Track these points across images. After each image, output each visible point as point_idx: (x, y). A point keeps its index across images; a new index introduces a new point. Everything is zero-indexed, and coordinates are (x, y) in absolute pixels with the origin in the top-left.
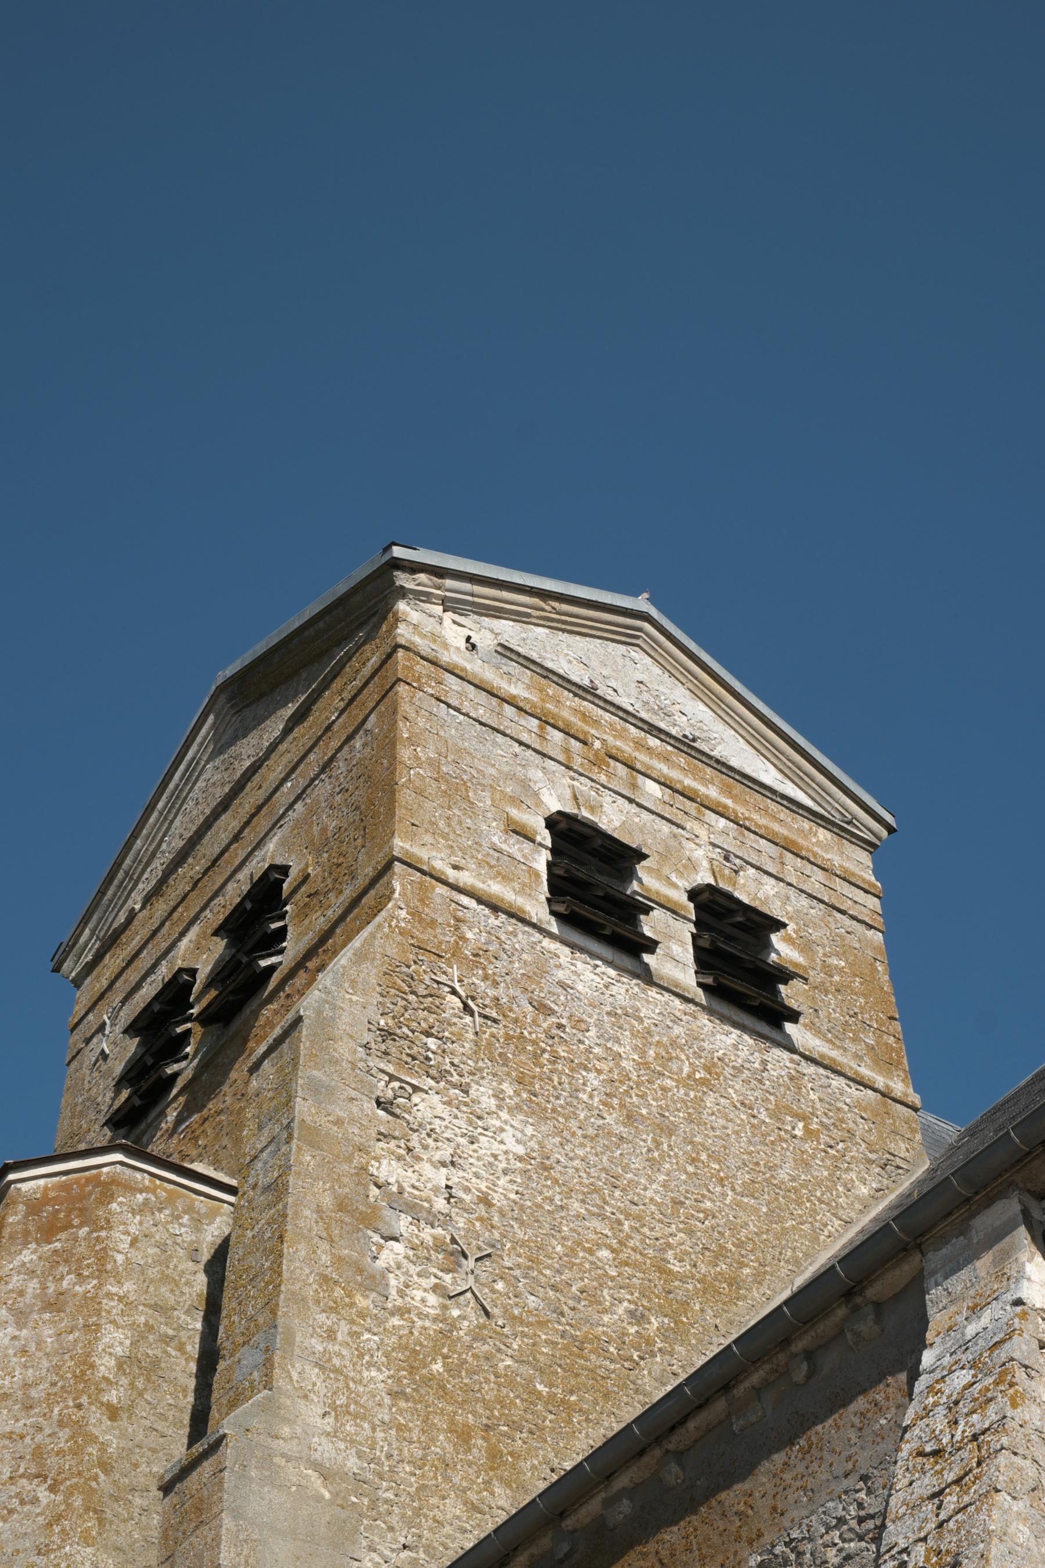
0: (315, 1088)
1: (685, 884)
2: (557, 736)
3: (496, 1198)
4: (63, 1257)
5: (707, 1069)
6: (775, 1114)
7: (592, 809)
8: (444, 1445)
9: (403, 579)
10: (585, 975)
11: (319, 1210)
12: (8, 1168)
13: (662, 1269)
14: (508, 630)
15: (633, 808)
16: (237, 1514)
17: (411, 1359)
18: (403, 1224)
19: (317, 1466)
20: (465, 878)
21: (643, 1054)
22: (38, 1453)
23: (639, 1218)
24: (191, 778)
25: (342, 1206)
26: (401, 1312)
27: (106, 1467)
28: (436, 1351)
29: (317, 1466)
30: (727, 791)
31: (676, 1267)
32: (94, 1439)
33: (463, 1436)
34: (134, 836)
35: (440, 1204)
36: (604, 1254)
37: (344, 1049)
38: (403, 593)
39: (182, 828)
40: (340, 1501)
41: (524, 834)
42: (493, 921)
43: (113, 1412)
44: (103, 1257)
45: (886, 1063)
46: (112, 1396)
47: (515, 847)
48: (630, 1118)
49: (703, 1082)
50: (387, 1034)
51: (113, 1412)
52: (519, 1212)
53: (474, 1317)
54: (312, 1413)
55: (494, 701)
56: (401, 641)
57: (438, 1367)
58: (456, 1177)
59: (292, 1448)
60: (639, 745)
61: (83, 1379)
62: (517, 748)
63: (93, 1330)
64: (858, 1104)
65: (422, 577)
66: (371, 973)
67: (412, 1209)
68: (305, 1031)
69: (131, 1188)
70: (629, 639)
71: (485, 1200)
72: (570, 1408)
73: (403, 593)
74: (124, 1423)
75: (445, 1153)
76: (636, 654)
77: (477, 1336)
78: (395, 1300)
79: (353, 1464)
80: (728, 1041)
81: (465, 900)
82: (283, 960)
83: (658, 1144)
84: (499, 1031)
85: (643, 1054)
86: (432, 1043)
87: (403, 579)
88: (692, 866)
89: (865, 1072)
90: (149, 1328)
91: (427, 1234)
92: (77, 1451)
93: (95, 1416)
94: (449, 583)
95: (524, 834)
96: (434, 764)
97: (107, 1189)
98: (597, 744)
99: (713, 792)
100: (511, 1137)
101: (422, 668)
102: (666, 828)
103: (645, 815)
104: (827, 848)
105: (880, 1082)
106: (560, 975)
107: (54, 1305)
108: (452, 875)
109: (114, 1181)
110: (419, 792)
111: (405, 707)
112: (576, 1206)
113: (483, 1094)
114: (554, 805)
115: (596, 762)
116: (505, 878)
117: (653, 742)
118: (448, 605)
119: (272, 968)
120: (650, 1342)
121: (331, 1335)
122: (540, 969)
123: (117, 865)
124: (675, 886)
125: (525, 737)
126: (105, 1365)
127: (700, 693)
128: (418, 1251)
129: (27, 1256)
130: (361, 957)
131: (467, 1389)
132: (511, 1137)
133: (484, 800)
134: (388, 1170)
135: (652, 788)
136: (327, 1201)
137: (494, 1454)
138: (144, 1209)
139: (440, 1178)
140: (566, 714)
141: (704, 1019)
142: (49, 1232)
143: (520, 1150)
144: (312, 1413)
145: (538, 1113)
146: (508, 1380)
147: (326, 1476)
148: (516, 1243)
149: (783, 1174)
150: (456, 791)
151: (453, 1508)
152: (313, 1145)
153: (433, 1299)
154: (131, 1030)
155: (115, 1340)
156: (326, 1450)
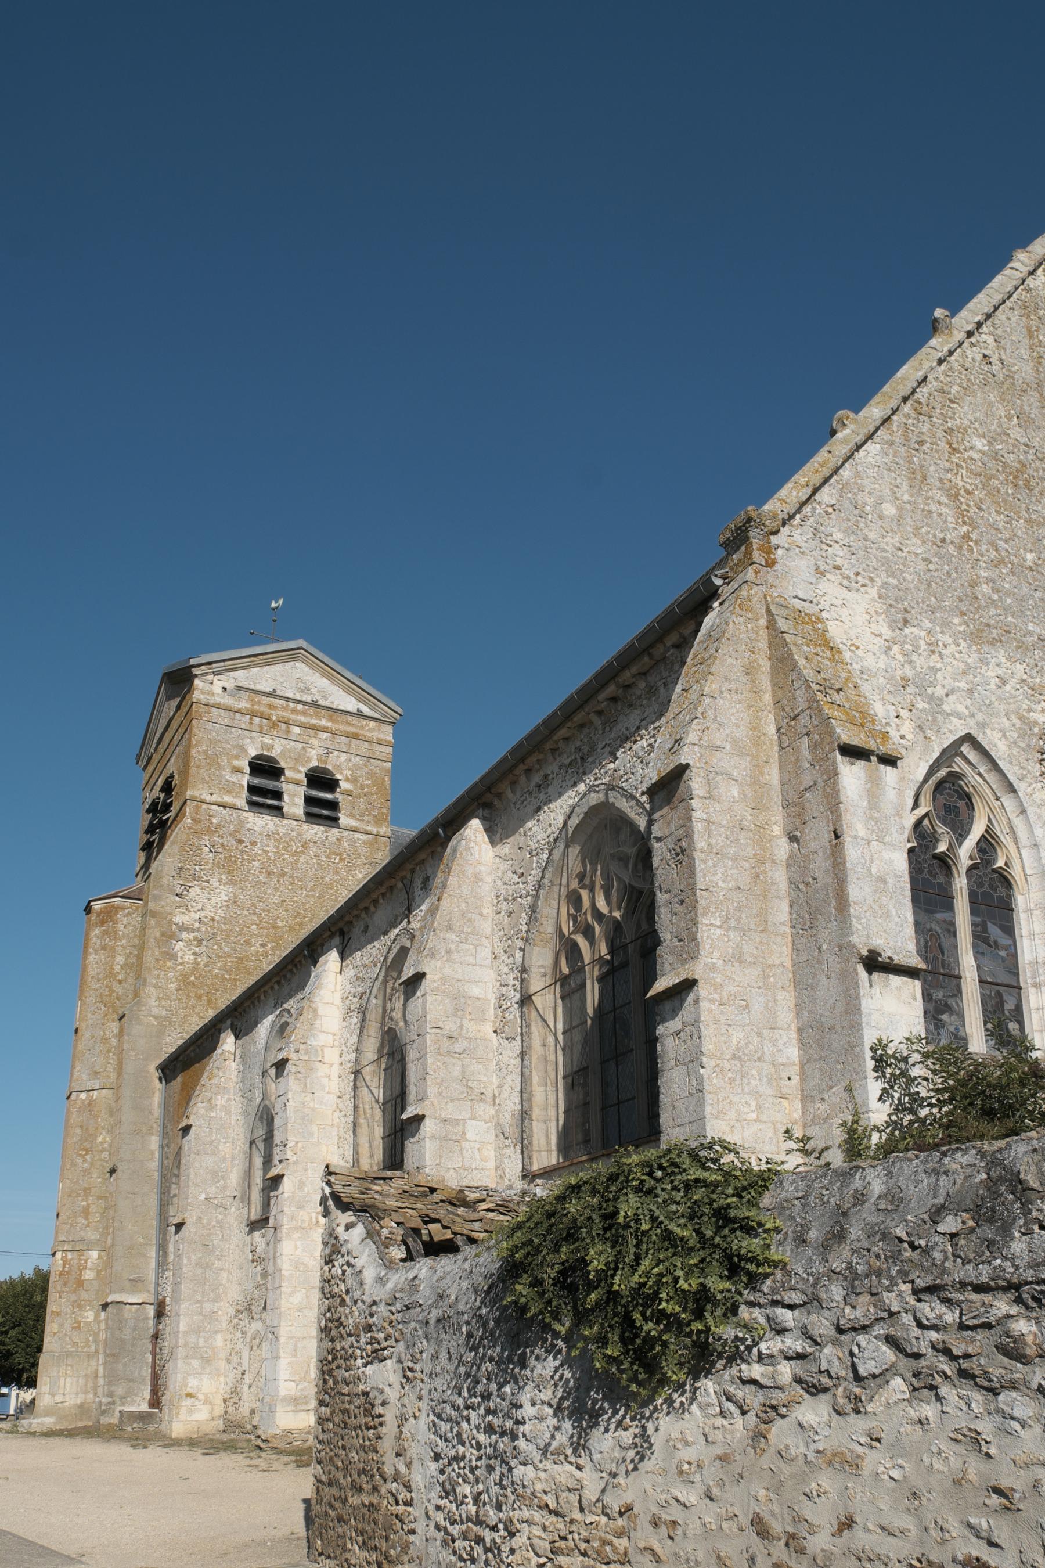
0: (155, 897)
1: (304, 770)
2: (257, 720)
3: (217, 918)
4: (105, 932)
5: (303, 846)
6: (328, 857)
7: (268, 750)
8: (193, 1001)
9: (196, 671)
10: (261, 822)
11: (155, 938)
12: (90, 902)
13: (275, 927)
14: (241, 677)
15: (287, 742)
16: (129, 1035)
17: (185, 977)
18: (184, 935)
19: (153, 1016)
20: (215, 798)
21: (278, 848)
22: (101, 995)
23: (268, 911)
24: (160, 712)
25: (163, 935)
26: (181, 964)
27: (118, 999)
28: (192, 973)
29: (153, 1016)
30: (330, 719)
31: (280, 924)
32: (114, 991)
33: (199, 997)
34: (149, 722)
35: (197, 925)
36: (254, 927)
37: (165, 881)
38: (196, 676)
39: (163, 722)
40: (160, 1024)
41: (238, 770)
42: (224, 812)
43: (120, 982)
44: (116, 933)
45: (378, 822)
46: (120, 977)
47: (234, 778)
48: (269, 874)
49: (301, 852)
50: (181, 869)
51: (120, 982)
52: (225, 920)
53: (205, 959)
54: (153, 1002)
55: (232, 714)
56: (194, 700)
57: (193, 978)
58: (203, 914)
59: (145, 1013)
60: (294, 711)
61: (111, 974)
62: (240, 731)
63: (113, 957)
64: (365, 843)
65: (203, 667)
66: (176, 849)
67: (187, 929)
68: (152, 878)
69: (123, 909)
70: (295, 659)
71: (213, 920)
72: (236, 980)
73: (196, 676)
74: (124, 984)
75: (200, 907)
76: (298, 664)
77: (206, 966)
78: (180, 960)
79: (164, 1013)
80: (315, 831)
81: (213, 807)
82: (171, 814)
83: (278, 881)
84: (222, 856)
85: (278, 848)
86: (197, 868)
87: (196, 671)
88: (309, 760)
89: (369, 828)
90: (131, 953)
91: (191, 936)
92: (110, 995)
93: (115, 986)
94: (214, 665)
95: (238, 770)
96: (205, 752)
97: (117, 909)
98: (274, 718)
99: (324, 722)
100: (223, 894)
101: (203, 709)
102: (300, 745)
103: (293, 743)
104: (371, 730)
105: (375, 830)
106: (248, 826)
107: (104, 948)
108: (208, 798)
109: (118, 907)
110: (198, 767)
111: (195, 730)
112: (246, 912)
113: (214, 882)
114: (253, 752)
115: (274, 726)
116: (229, 792)
117: (300, 707)
118: (215, 674)
119: (168, 819)
120: (267, 953)
121: (158, 977)
122: (241, 823)
123: (147, 731)
124: (300, 772)
125: (243, 726)
126: (117, 968)
127: (324, 675)
128: (189, 943)
129: (97, 931)
130: (173, 843)
131: (201, 983)
132: (223, 894)
133: (224, 761)
134: (179, 919)
135: (296, 730)
136: (158, 934)
137: (209, 1001)
138: (129, 914)
139: (197, 916)
140: (263, 709)
141: (305, 826)
142: (103, 923)
143: (226, 898)
144: (153, 1002)
145: (232, 882)
146: (217, 976)
147: (156, 1018)
148: (222, 931)
149: (327, 879)
150: (213, 761)
151: (195, 1019)
152: (153, 917)
153: (192, 957)
154: (148, 811)
155: (120, 960)
156: (155, 1011)
